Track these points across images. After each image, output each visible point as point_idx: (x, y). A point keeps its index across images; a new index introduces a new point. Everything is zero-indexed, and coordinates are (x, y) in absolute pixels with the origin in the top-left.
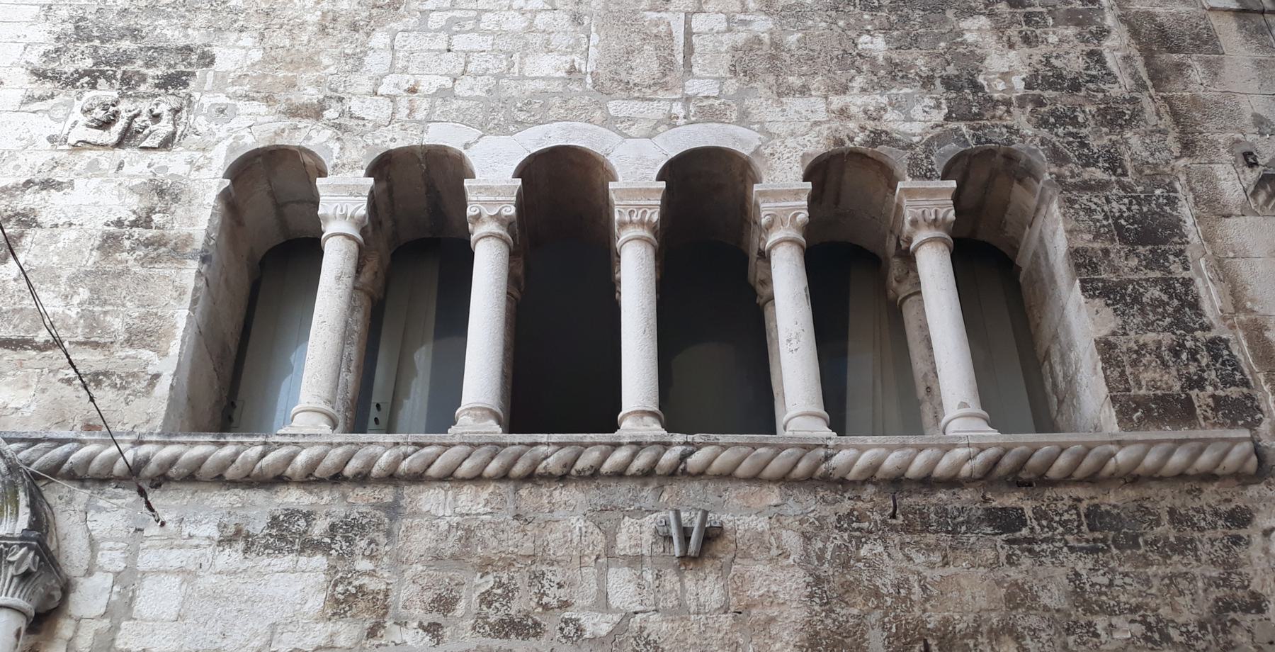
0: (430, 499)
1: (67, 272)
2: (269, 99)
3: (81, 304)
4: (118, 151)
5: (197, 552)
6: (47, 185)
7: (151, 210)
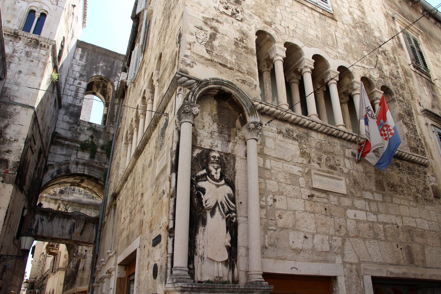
0: (313, 134)
1: (229, 49)
3: (235, 59)
4: (231, 18)
5: (273, 134)
6: (217, 21)
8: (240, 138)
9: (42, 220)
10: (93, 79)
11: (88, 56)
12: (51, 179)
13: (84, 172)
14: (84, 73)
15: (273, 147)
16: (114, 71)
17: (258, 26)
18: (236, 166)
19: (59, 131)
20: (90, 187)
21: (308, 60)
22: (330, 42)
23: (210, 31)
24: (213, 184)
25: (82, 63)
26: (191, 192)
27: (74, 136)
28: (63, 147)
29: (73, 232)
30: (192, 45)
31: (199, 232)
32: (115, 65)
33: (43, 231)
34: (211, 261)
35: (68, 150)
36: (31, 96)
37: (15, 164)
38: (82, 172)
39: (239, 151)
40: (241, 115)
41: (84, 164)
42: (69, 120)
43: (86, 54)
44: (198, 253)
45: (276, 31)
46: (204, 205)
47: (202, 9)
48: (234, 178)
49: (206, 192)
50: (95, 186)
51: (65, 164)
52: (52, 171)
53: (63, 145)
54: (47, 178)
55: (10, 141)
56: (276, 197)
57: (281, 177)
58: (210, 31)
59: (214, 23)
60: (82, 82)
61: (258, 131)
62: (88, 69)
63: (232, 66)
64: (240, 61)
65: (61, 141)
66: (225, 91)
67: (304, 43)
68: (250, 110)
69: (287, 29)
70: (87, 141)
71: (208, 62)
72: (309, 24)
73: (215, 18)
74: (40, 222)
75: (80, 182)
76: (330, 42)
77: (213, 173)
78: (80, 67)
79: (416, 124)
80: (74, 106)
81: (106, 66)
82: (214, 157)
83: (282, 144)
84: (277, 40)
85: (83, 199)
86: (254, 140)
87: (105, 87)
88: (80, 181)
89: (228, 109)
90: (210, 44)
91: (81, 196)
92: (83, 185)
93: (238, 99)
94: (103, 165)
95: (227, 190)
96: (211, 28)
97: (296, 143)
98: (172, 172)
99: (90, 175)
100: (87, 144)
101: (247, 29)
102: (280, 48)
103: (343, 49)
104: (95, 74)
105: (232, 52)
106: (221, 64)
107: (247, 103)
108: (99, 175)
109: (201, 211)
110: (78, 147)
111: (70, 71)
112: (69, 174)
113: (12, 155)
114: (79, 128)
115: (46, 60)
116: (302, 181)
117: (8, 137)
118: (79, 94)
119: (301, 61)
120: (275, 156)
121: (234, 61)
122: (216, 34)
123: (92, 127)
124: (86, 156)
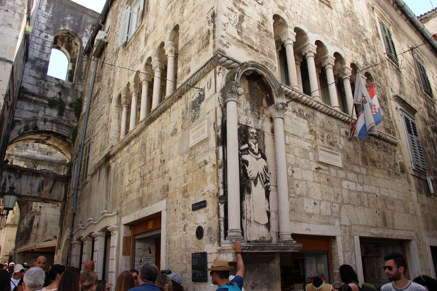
1: (254, 32)
8: (267, 116)
9: (10, 177)
10: (60, 34)
11: (54, 7)
12: (18, 135)
13: (52, 129)
14: (51, 26)
15: (290, 125)
16: (82, 26)
17: (274, 11)
18: (265, 141)
19: (24, 85)
20: (56, 144)
21: (313, 45)
22: (328, 29)
23: (239, 13)
24: (254, 157)
25: (48, 14)
26: (240, 165)
27: (42, 92)
28: (31, 102)
29: (42, 189)
30: (226, 26)
31: (246, 199)
32: (83, 20)
34: (257, 224)
35: (36, 106)
36: (8, 49)
38: (50, 130)
40: (268, 95)
41: (52, 122)
42: (36, 75)
43: (52, 5)
44: (245, 217)
45: (287, 15)
46: (249, 176)
48: (265, 152)
49: (249, 164)
50: (61, 144)
51: (32, 120)
52: (19, 128)
53: (30, 101)
54: (14, 134)
56: (294, 169)
57: (296, 151)
58: (239, 13)
59: (241, 5)
60: (49, 36)
61: (284, 111)
62: (55, 22)
63: (258, 48)
64: (263, 44)
65: (28, 96)
66: (259, 73)
67: (308, 29)
68: (278, 91)
69: (296, 15)
70: (55, 97)
71: (239, 43)
72: (312, 11)
74: (8, 180)
75: (45, 139)
76: (328, 29)
77: (253, 147)
79: (389, 108)
80: (41, 60)
81: (74, 21)
82: (253, 133)
83: (296, 122)
84: (288, 25)
85: (37, 155)
86: (281, 119)
87: (69, 41)
88: (46, 138)
89: (256, 88)
91: (35, 152)
92: (49, 142)
93: (268, 81)
94: (71, 123)
96: (239, 10)
97: (306, 121)
98: (218, 145)
99: (59, 132)
100: (56, 101)
101: (266, 13)
102: (291, 33)
103: (337, 36)
104: (62, 28)
105: (257, 35)
106: (249, 46)
107: (276, 86)
108: (68, 133)
109: (245, 181)
110: (45, 104)
111: (36, 22)
112: (36, 131)
114: (47, 83)
115: (23, 11)
116: (311, 154)
119: (306, 46)
120: (292, 132)
121: (258, 43)
123: (59, 83)
124: (54, 113)
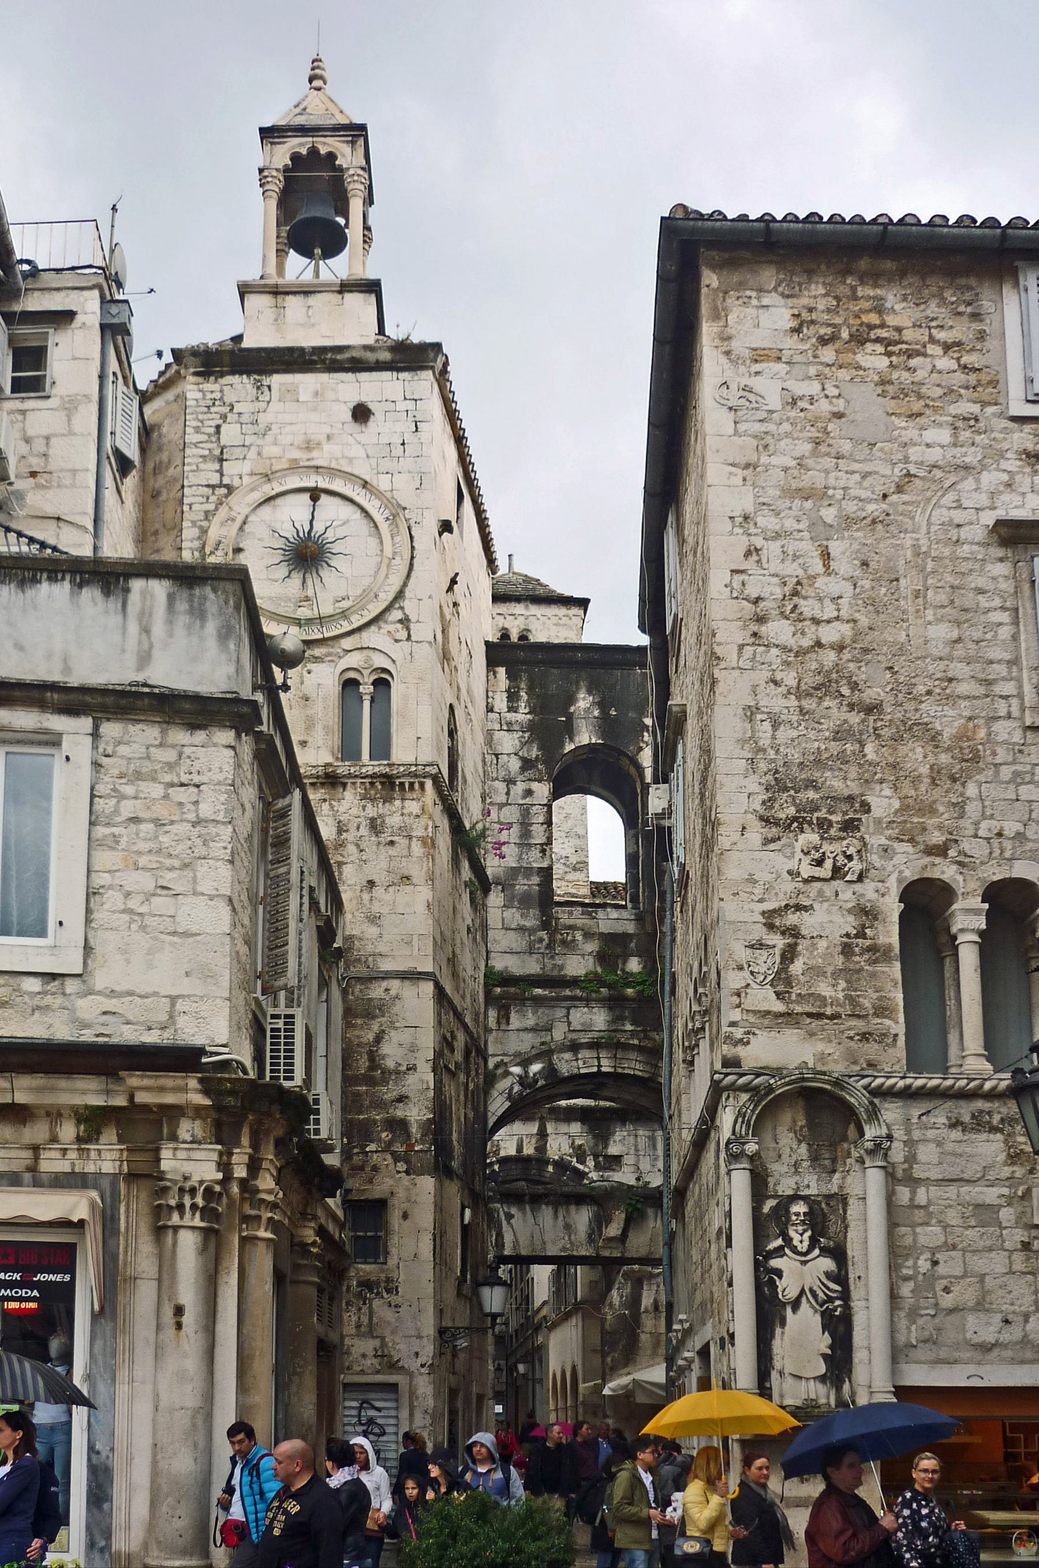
1: (830, 970)
2: (911, 840)
6: (798, 908)
7: (863, 927)
13: (599, 1066)
14: (534, 752)
27: (549, 966)
29: (600, 1236)
33: (516, 1243)
35: (540, 1011)
37: (425, 1126)
38: (595, 1069)
39: (853, 1185)
41: (595, 1045)
47: (758, 891)
55: (398, 1072)
59: (790, 916)
60: (535, 786)
63: (839, 1009)
73: (792, 902)
78: (516, 735)
80: (528, 871)
90: (783, 976)
95: (827, 1264)
96: (783, 933)
99: (620, 1070)
113: (411, 1105)
117: (390, 1064)
118: (533, 828)
122: (796, 944)
